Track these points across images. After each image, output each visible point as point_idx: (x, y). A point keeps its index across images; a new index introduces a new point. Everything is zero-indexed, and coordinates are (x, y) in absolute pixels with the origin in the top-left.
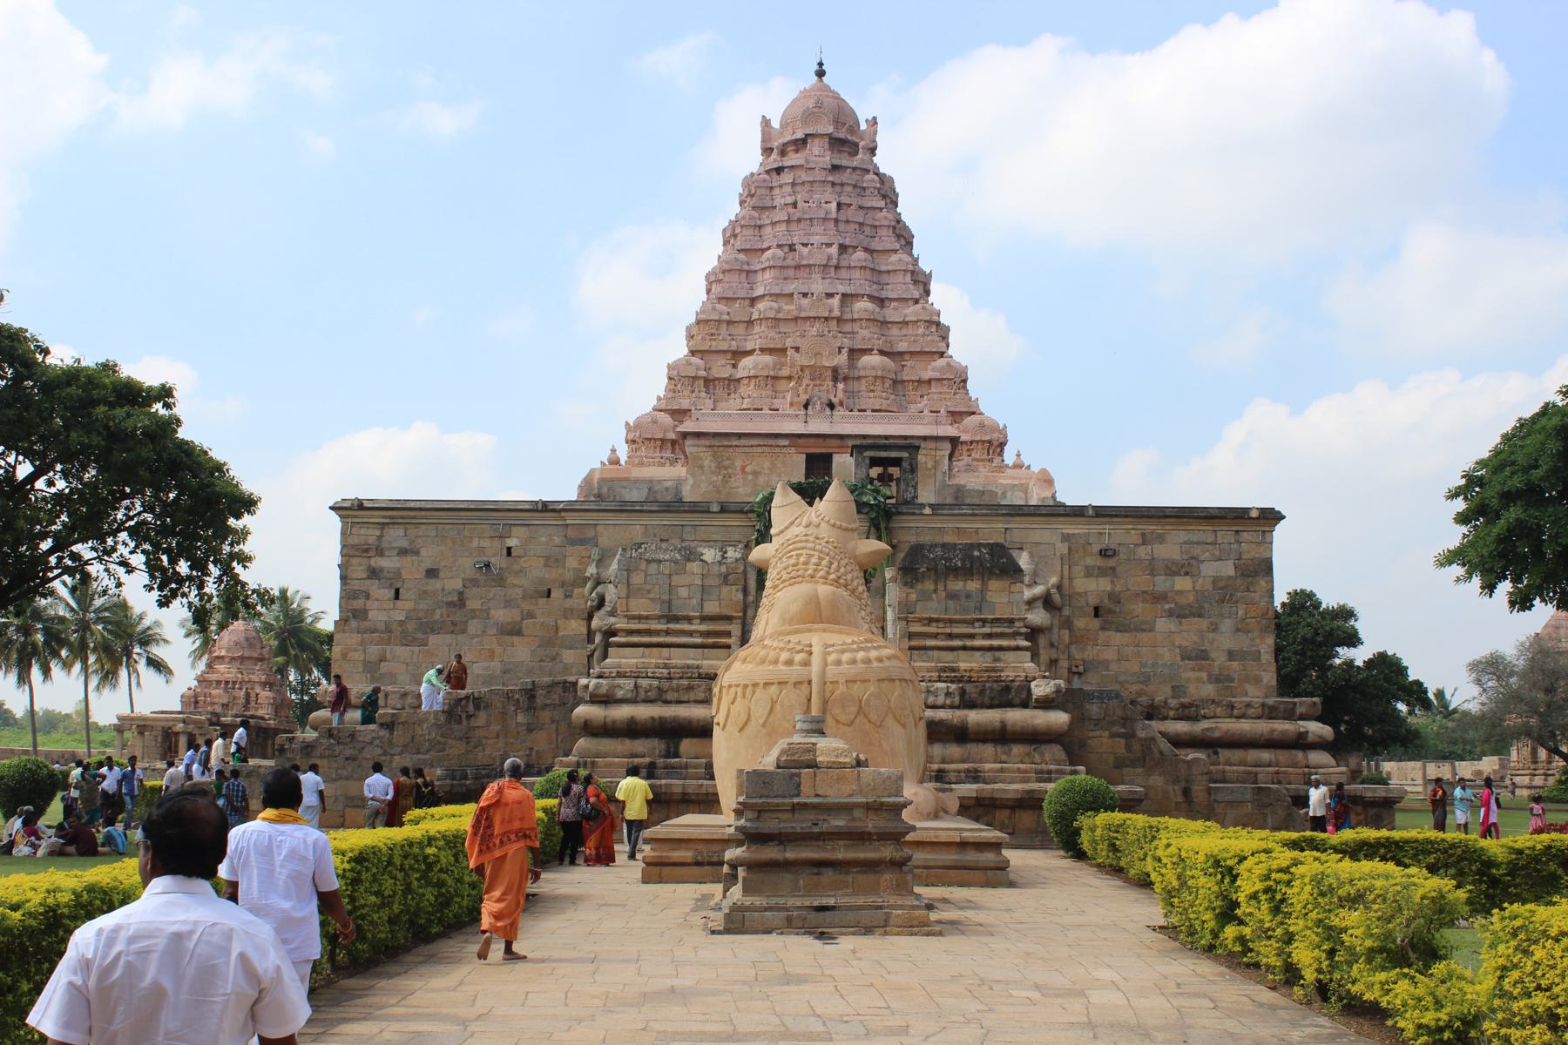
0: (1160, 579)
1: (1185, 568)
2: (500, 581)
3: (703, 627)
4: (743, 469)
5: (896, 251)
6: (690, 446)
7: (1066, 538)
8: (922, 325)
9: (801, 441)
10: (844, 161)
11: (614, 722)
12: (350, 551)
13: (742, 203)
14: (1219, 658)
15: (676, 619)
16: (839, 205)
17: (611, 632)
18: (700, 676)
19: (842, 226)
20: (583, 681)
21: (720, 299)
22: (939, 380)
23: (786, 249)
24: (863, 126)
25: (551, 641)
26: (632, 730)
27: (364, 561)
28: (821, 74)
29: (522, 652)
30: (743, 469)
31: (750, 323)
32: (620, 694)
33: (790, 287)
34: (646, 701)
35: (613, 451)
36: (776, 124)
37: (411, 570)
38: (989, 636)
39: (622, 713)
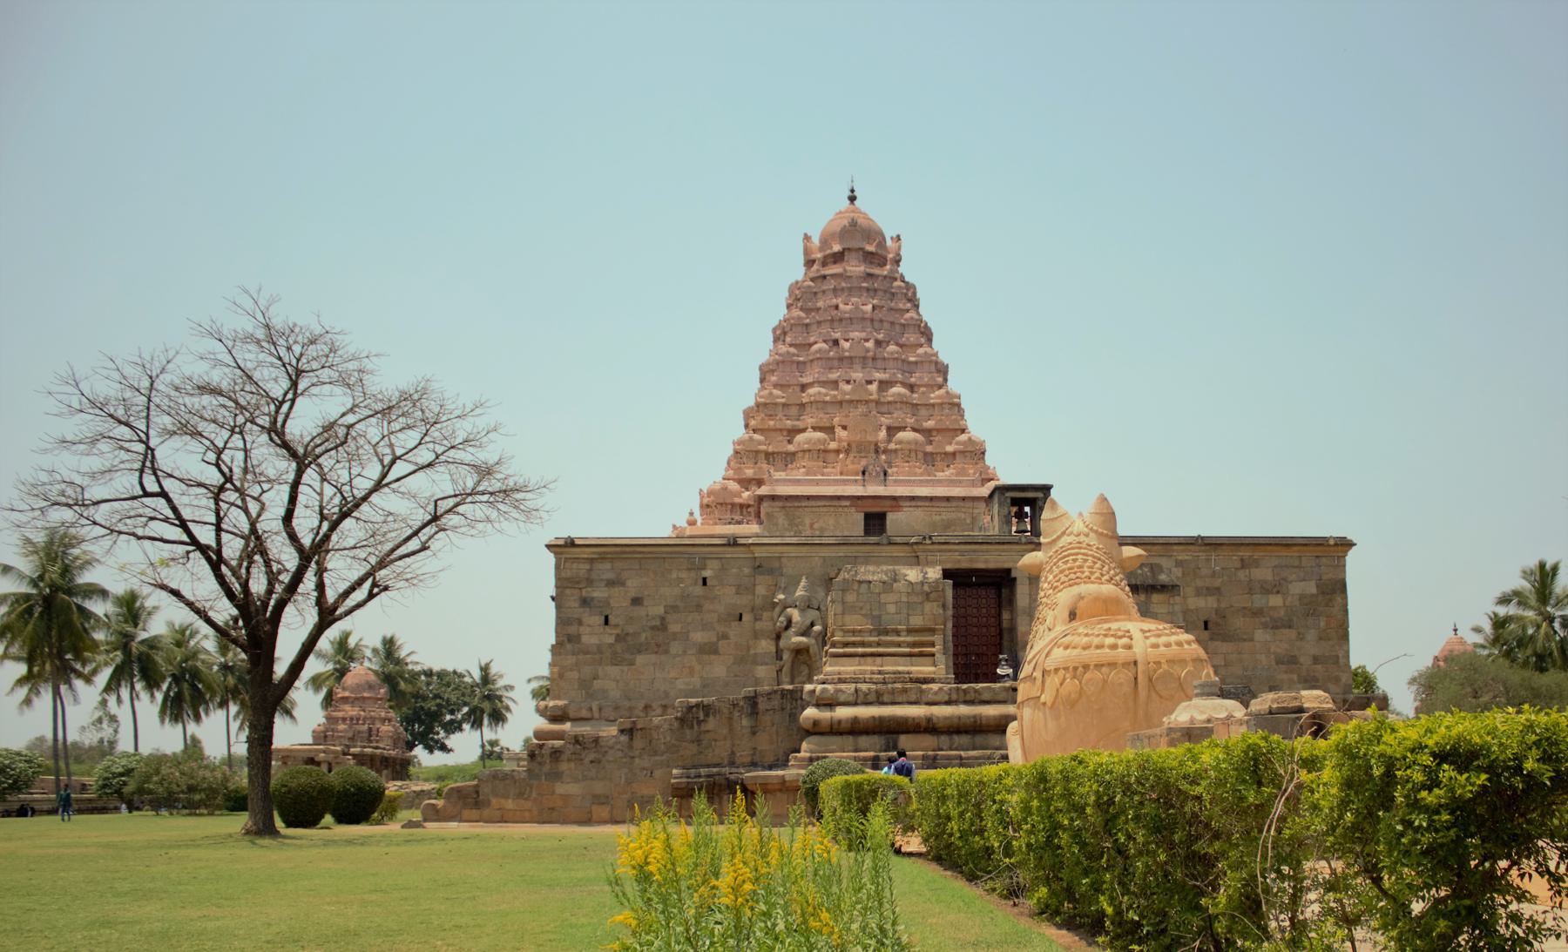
0: (1257, 597)
1: (1277, 588)
2: (699, 607)
3: (909, 639)
4: (811, 525)
7: (1179, 564)
10: (876, 271)
11: (840, 722)
12: (566, 587)
13: (789, 306)
14: (1305, 661)
15: (886, 632)
16: (874, 308)
18: (912, 681)
19: (877, 325)
20: (808, 687)
21: (776, 386)
22: (963, 452)
24: (889, 243)
25: (745, 659)
26: (855, 729)
27: (576, 592)
28: (852, 199)
29: (718, 669)
30: (811, 525)
31: (802, 406)
32: (842, 698)
33: (834, 376)
34: (867, 703)
35: (691, 514)
36: (816, 240)
37: (619, 600)
39: (843, 713)
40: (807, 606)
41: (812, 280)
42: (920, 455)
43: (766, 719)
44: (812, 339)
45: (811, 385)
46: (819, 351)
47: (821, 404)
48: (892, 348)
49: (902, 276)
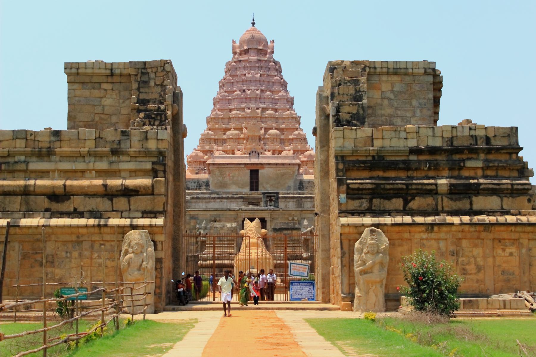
4: (229, 175)
5: (281, 91)
6: (211, 167)
8: (290, 119)
9: (248, 166)
13: (226, 72)
15: (221, 241)
16: (261, 75)
17: (204, 243)
21: (219, 110)
22: (296, 139)
23: (242, 91)
24: (269, 43)
28: (253, 24)
30: (229, 175)
33: (243, 106)
36: (238, 43)
38: (293, 244)
40: (206, 228)
41: (235, 62)
42: (278, 140)
43: (190, 263)
44: (235, 89)
45: (233, 109)
46: (237, 95)
47: (238, 118)
48: (268, 93)
49: (274, 60)
